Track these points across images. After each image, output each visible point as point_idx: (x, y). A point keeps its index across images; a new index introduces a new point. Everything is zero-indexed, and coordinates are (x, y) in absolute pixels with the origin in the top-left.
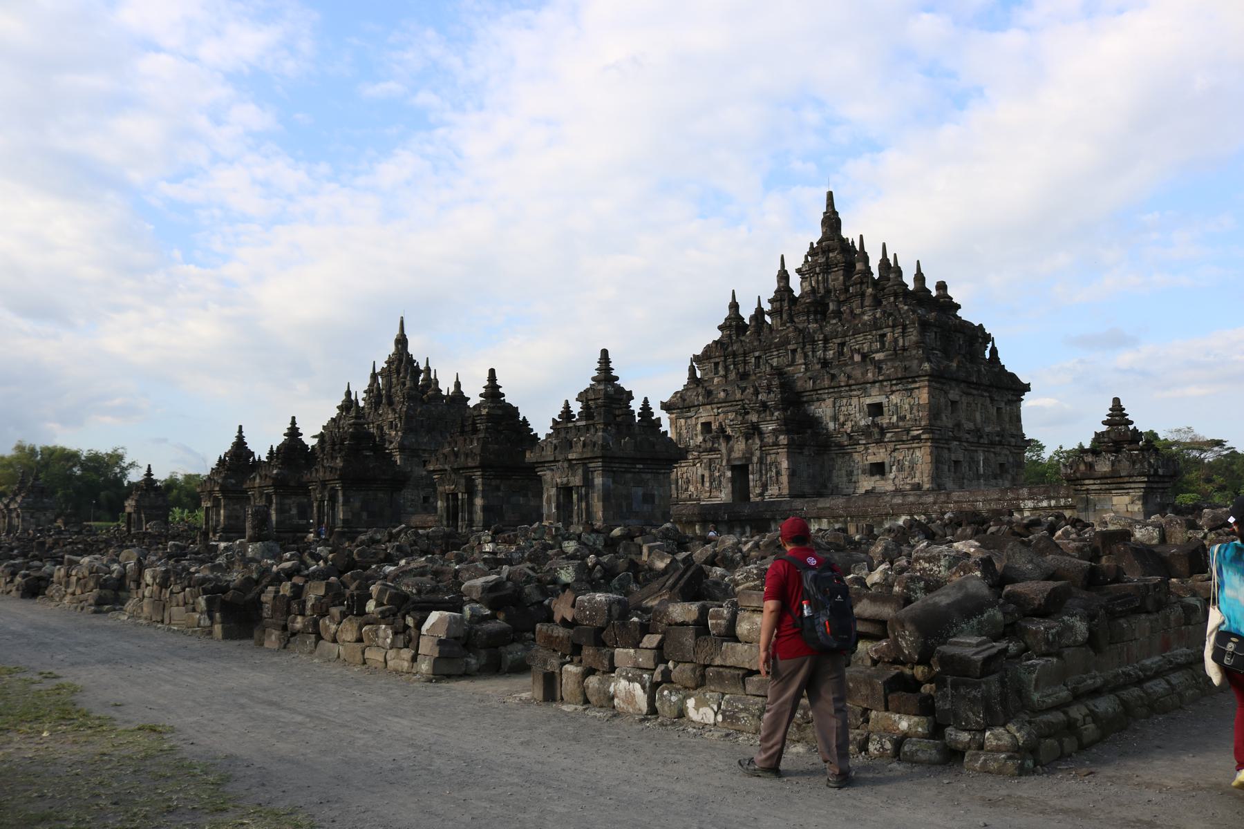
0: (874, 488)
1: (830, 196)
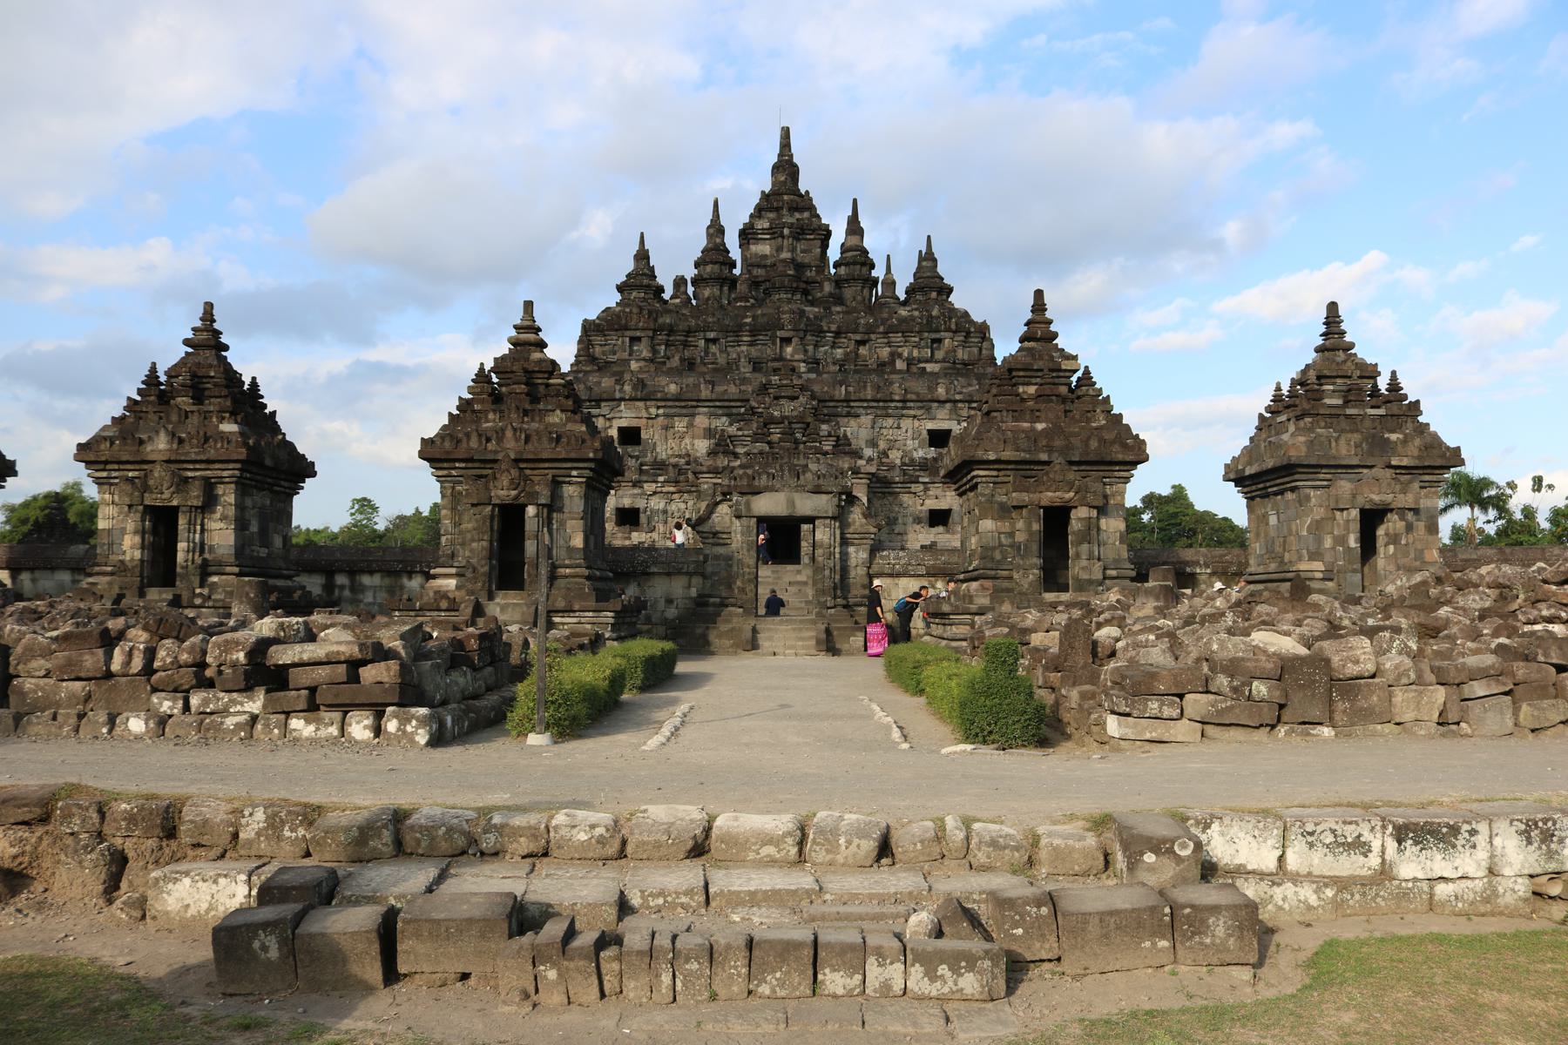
0: (934, 544)
1: (786, 133)
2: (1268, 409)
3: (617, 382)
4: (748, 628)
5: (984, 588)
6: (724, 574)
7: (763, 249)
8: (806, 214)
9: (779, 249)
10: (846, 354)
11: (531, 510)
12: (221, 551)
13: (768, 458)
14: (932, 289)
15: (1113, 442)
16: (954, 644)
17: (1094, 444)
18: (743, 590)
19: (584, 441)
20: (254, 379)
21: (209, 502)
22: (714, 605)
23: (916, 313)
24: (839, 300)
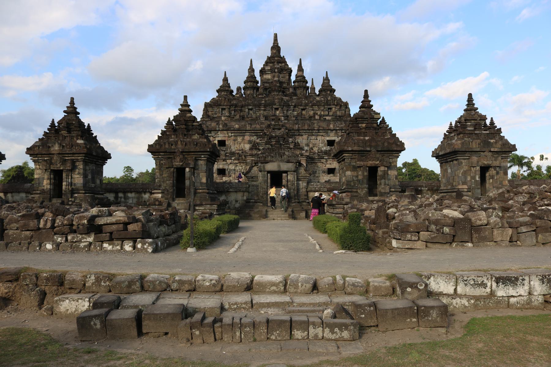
0: (329, 180)
1: (276, 36)
2: (447, 131)
3: (217, 124)
4: (264, 210)
5: (347, 196)
6: (256, 191)
7: (268, 76)
8: (283, 64)
9: (274, 77)
10: (298, 114)
11: (187, 170)
12: (78, 185)
13: (271, 150)
14: (328, 90)
15: (393, 144)
16: (337, 215)
17: (386, 144)
18: (262, 197)
19: (206, 145)
20: (89, 124)
21: (74, 168)
22: (252, 202)
23: (323, 99)
24: (295, 95)
